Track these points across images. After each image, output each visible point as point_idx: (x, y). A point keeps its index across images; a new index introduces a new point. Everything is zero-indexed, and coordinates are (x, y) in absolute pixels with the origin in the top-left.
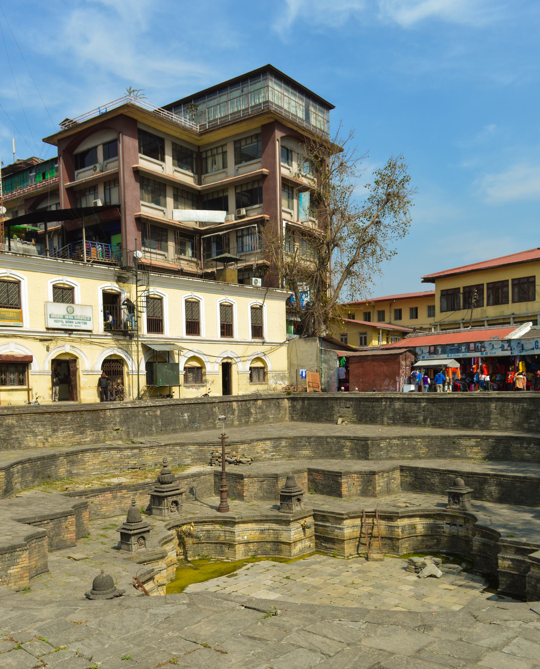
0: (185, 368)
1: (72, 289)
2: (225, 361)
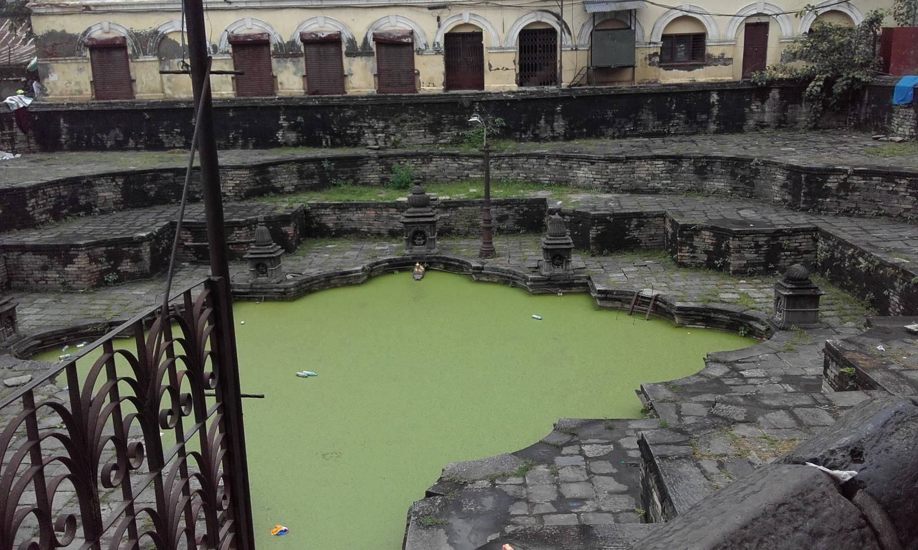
0: (664, 37)
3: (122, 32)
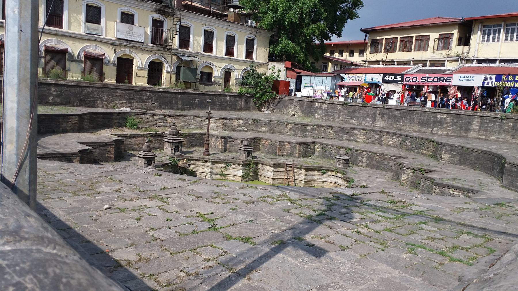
0: (201, 72)
1: (132, 16)
2: (227, 71)
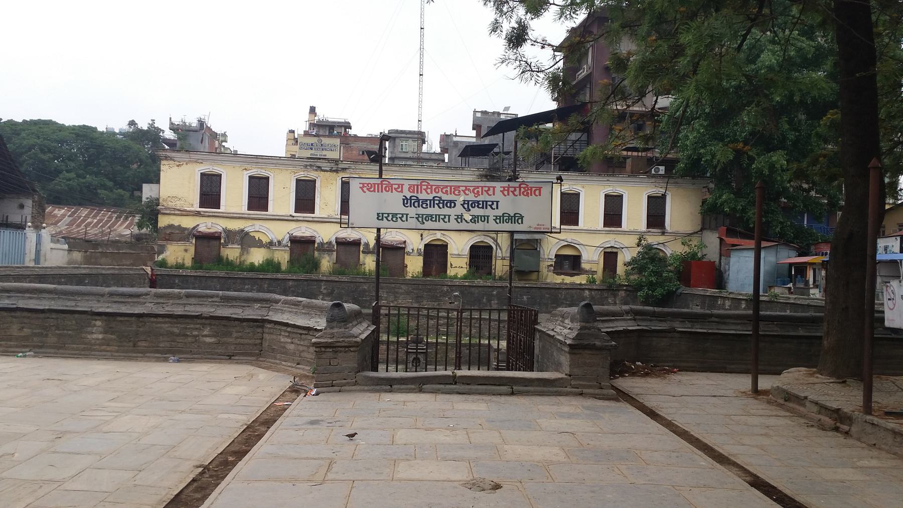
2: (609, 250)
3: (220, 229)
